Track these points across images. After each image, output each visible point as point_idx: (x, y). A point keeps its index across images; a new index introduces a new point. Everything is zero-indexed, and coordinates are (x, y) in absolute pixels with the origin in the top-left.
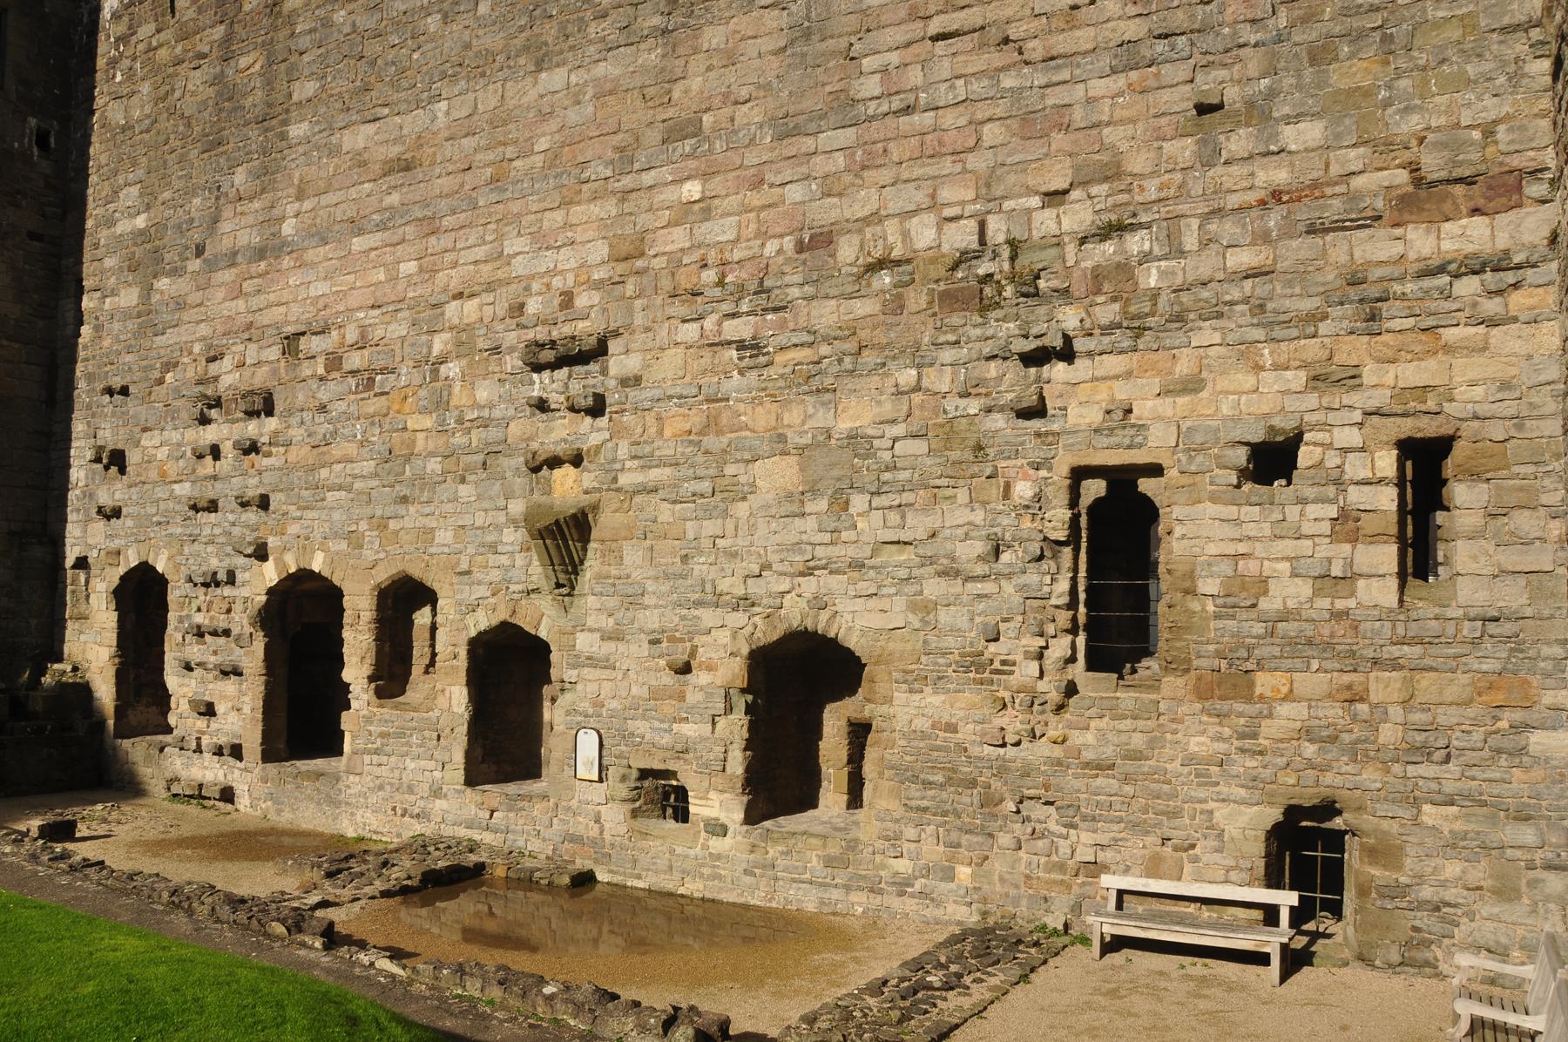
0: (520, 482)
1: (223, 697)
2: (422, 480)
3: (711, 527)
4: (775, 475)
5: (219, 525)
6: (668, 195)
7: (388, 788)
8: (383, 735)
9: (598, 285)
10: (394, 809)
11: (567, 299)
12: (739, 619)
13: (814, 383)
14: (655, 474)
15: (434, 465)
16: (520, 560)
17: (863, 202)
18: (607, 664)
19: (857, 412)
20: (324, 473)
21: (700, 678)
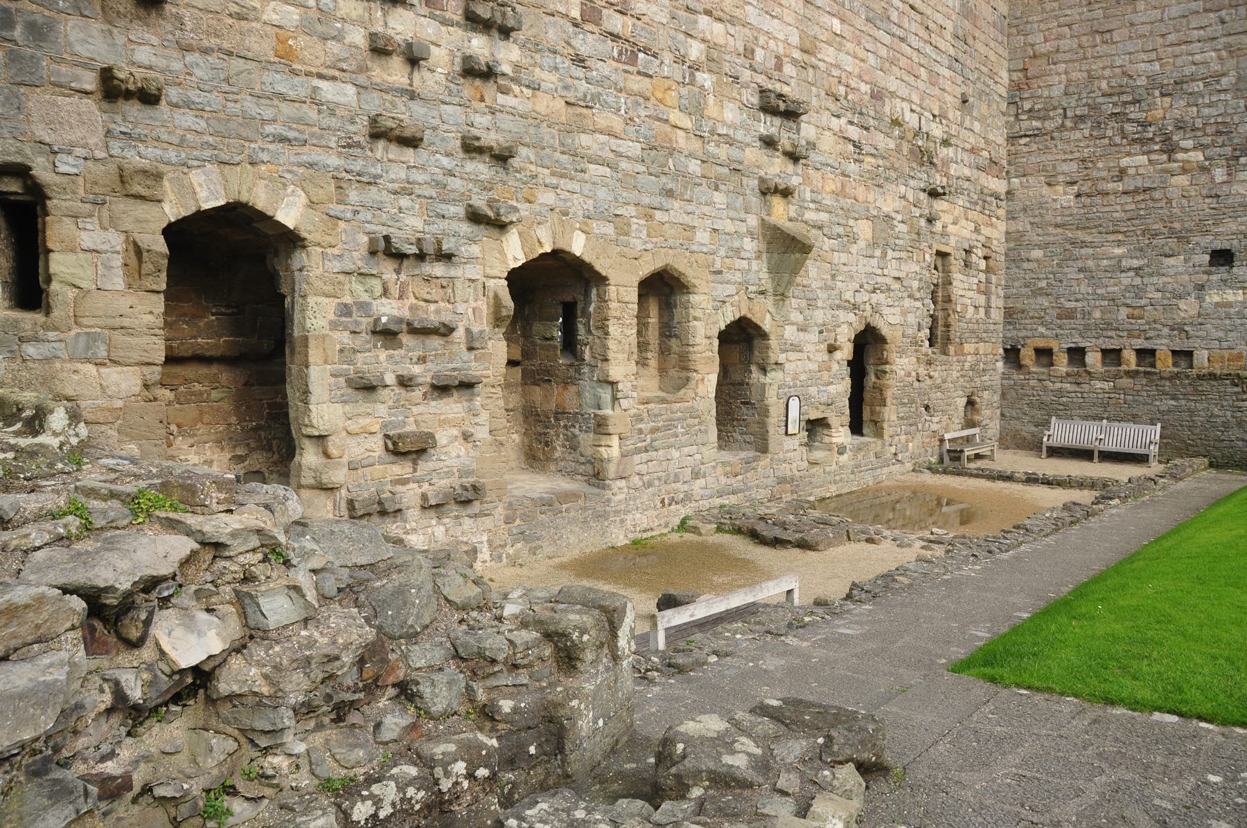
0: (755, 201)
1: (443, 423)
2: (681, 174)
3: (844, 257)
4: (864, 229)
5: (422, 168)
6: (826, 19)
7: (656, 483)
8: (654, 431)
9: (794, 62)
10: (663, 502)
11: (779, 67)
12: (851, 317)
13: (877, 181)
14: (824, 217)
15: (694, 167)
16: (755, 265)
17: (892, 84)
18: (796, 348)
19: (889, 205)
20: (585, 140)
21: (838, 355)
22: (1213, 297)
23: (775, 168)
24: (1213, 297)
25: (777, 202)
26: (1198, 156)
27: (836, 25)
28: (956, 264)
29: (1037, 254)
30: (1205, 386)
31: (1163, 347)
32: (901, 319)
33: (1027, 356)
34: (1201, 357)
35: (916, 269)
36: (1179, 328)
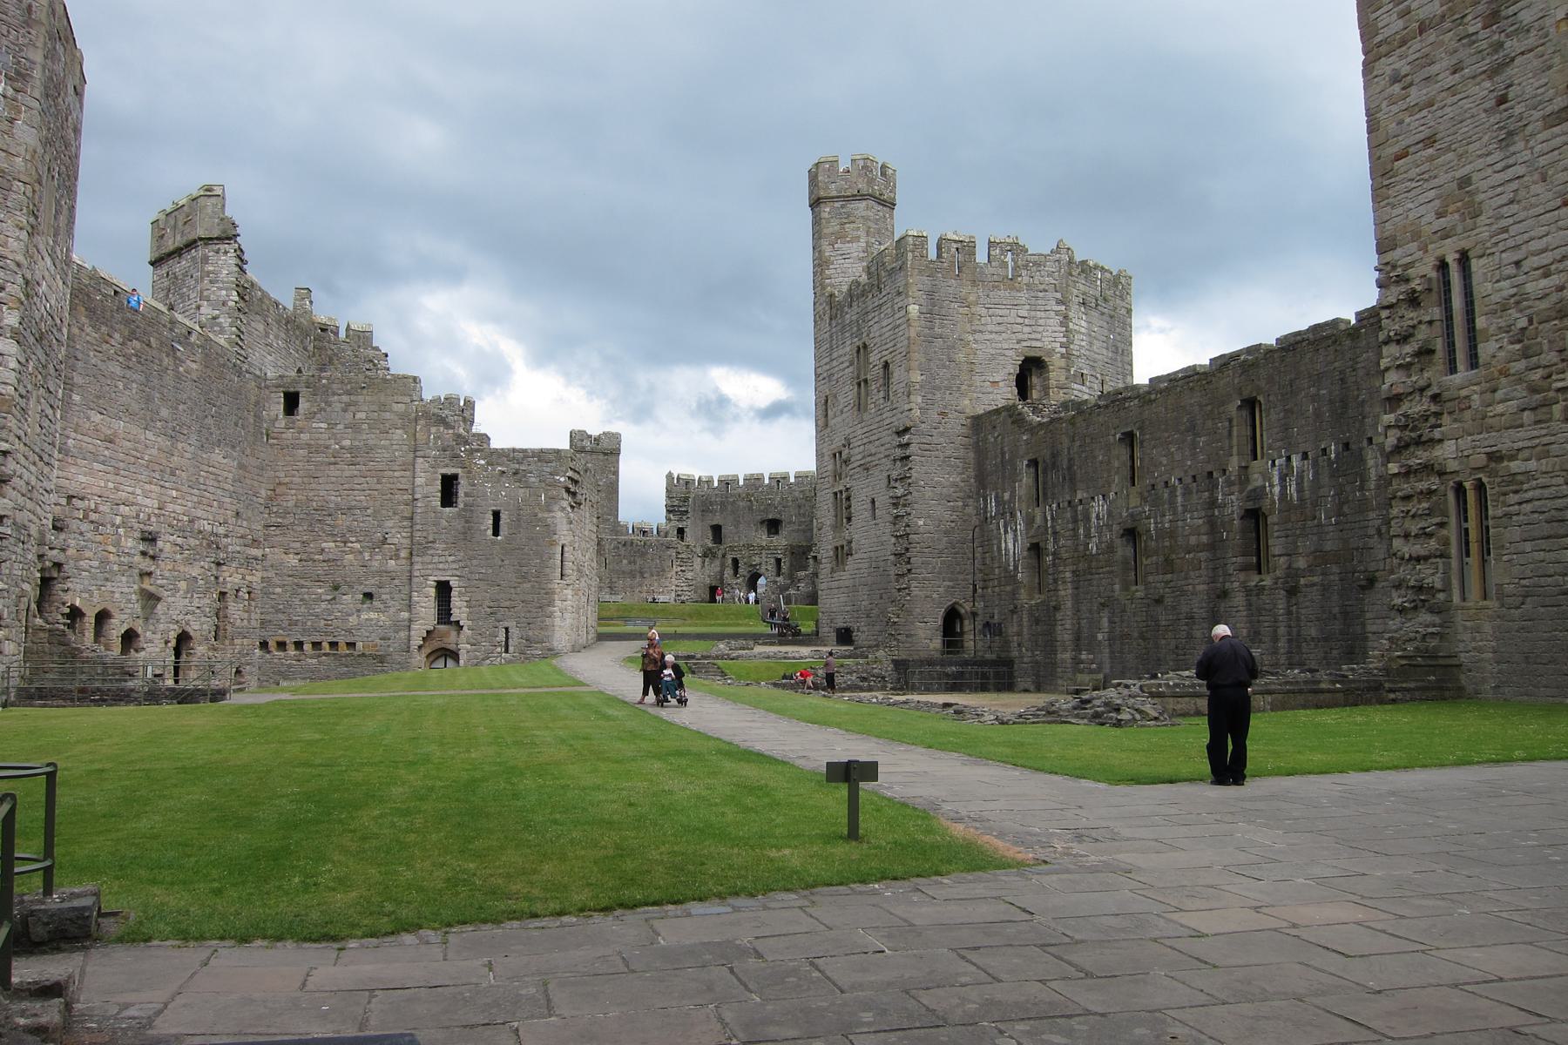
2: (111, 571)
4: (183, 585)
13: (189, 562)
15: (116, 568)
17: (200, 513)
18: (151, 641)
22: (364, 616)
23: (146, 564)
24: (364, 616)
25: (146, 579)
26: (357, 546)
27: (174, 493)
28: (230, 598)
29: (278, 590)
30: (361, 660)
31: (342, 640)
32: (199, 627)
33: (272, 644)
34: (359, 645)
35: (208, 602)
36: (349, 631)
